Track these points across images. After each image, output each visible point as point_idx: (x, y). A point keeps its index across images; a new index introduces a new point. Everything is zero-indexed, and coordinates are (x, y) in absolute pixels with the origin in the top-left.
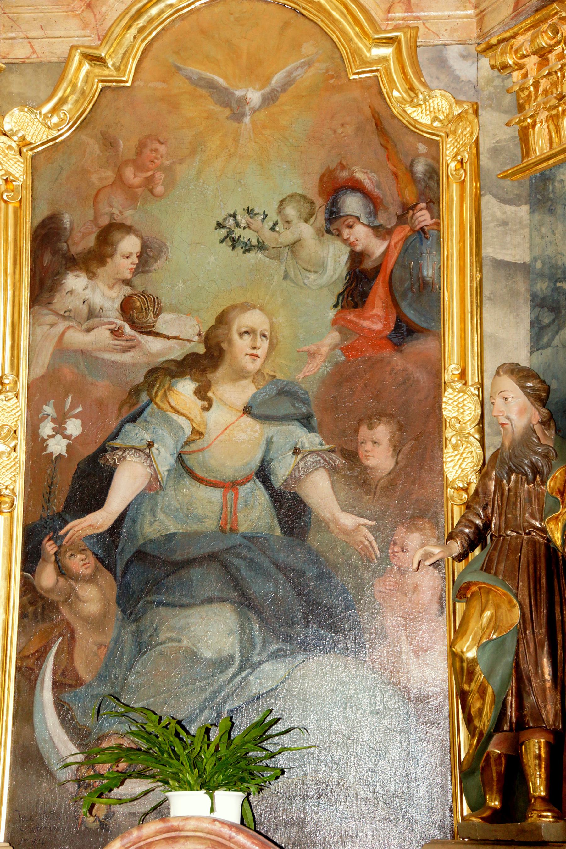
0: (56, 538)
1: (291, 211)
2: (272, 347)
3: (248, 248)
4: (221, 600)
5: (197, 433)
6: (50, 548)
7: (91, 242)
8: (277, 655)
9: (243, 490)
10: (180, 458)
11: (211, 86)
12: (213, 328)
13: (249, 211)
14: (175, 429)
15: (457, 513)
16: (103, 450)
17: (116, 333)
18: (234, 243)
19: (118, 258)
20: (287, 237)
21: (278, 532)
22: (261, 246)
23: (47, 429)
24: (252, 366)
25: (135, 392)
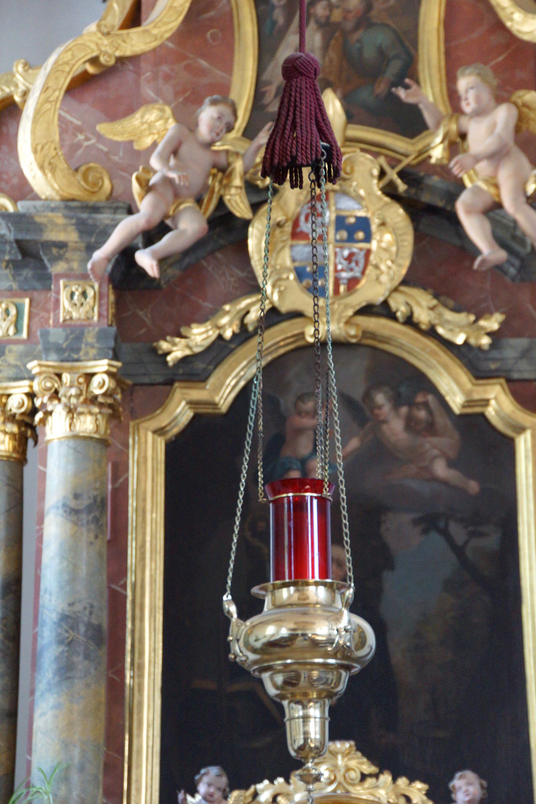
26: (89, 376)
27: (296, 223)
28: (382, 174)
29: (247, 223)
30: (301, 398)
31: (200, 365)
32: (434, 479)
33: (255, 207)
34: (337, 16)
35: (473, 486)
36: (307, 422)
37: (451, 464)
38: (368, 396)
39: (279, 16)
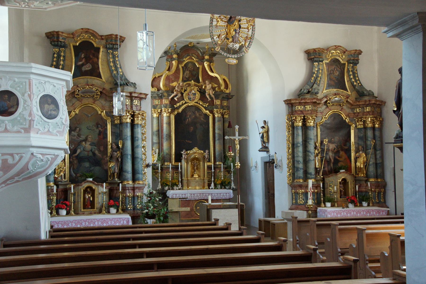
0: (72, 156)
1: (93, 126)
2: (92, 139)
3: (89, 130)
4: (88, 162)
5: (85, 147)
6: (71, 157)
7: (74, 129)
8: (93, 167)
9: (90, 152)
10: (83, 149)
11: (86, 114)
12: (86, 137)
13: (90, 126)
14: (83, 146)
15: (109, 155)
16: (76, 148)
17: (77, 137)
18: (88, 129)
19: (77, 130)
20: (93, 129)
21: (93, 156)
22: (91, 129)
23: (71, 146)
24: (90, 141)
25: (79, 143)
26: (168, 110)
27: (188, 93)
28: (197, 89)
29: (183, 93)
30: (188, 111)
31: (178, 108)
32: (201, 120)
33: (184, 91)
34: (191, 70)
35: (205, 121)
36: (189, 114)
37: (203, 119)
38: (195, 111)
39: (185, 70)
